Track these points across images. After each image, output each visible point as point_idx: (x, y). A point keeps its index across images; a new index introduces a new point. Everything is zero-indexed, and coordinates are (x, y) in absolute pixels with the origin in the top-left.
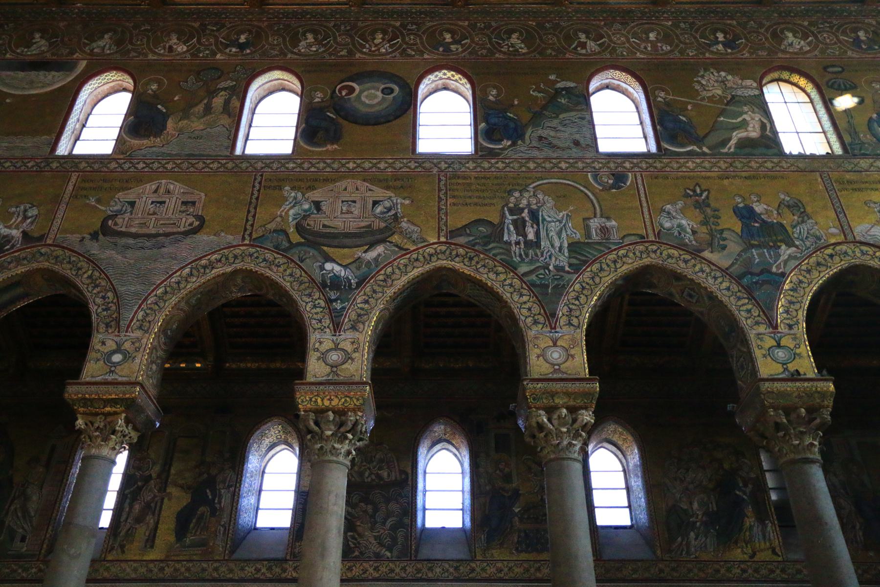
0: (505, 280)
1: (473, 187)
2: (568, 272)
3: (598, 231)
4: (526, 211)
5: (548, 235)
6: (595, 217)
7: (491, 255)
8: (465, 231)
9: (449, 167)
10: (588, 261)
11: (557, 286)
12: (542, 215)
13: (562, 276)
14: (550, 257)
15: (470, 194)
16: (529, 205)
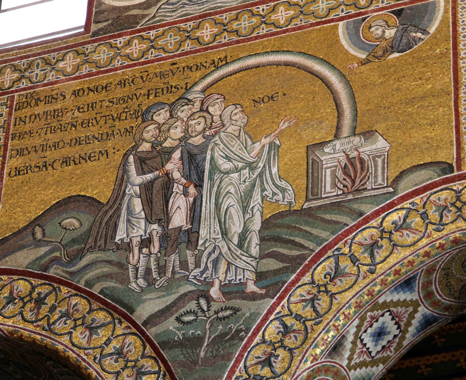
0: (108, 342)
1: (67, 118)
2: (254, 297)
3: (340, 173)
4: (177, 155)
5: (218, 206)
6: (337, 136)
7: (81, 285)
8: (33, 234)
9: (19, 80)
10: (304, 258)
11: (222, 336)
12: (212, 158)
13: (236, 310)
14: (216, 263)
15: (53, 138)
16: (184, 139)
